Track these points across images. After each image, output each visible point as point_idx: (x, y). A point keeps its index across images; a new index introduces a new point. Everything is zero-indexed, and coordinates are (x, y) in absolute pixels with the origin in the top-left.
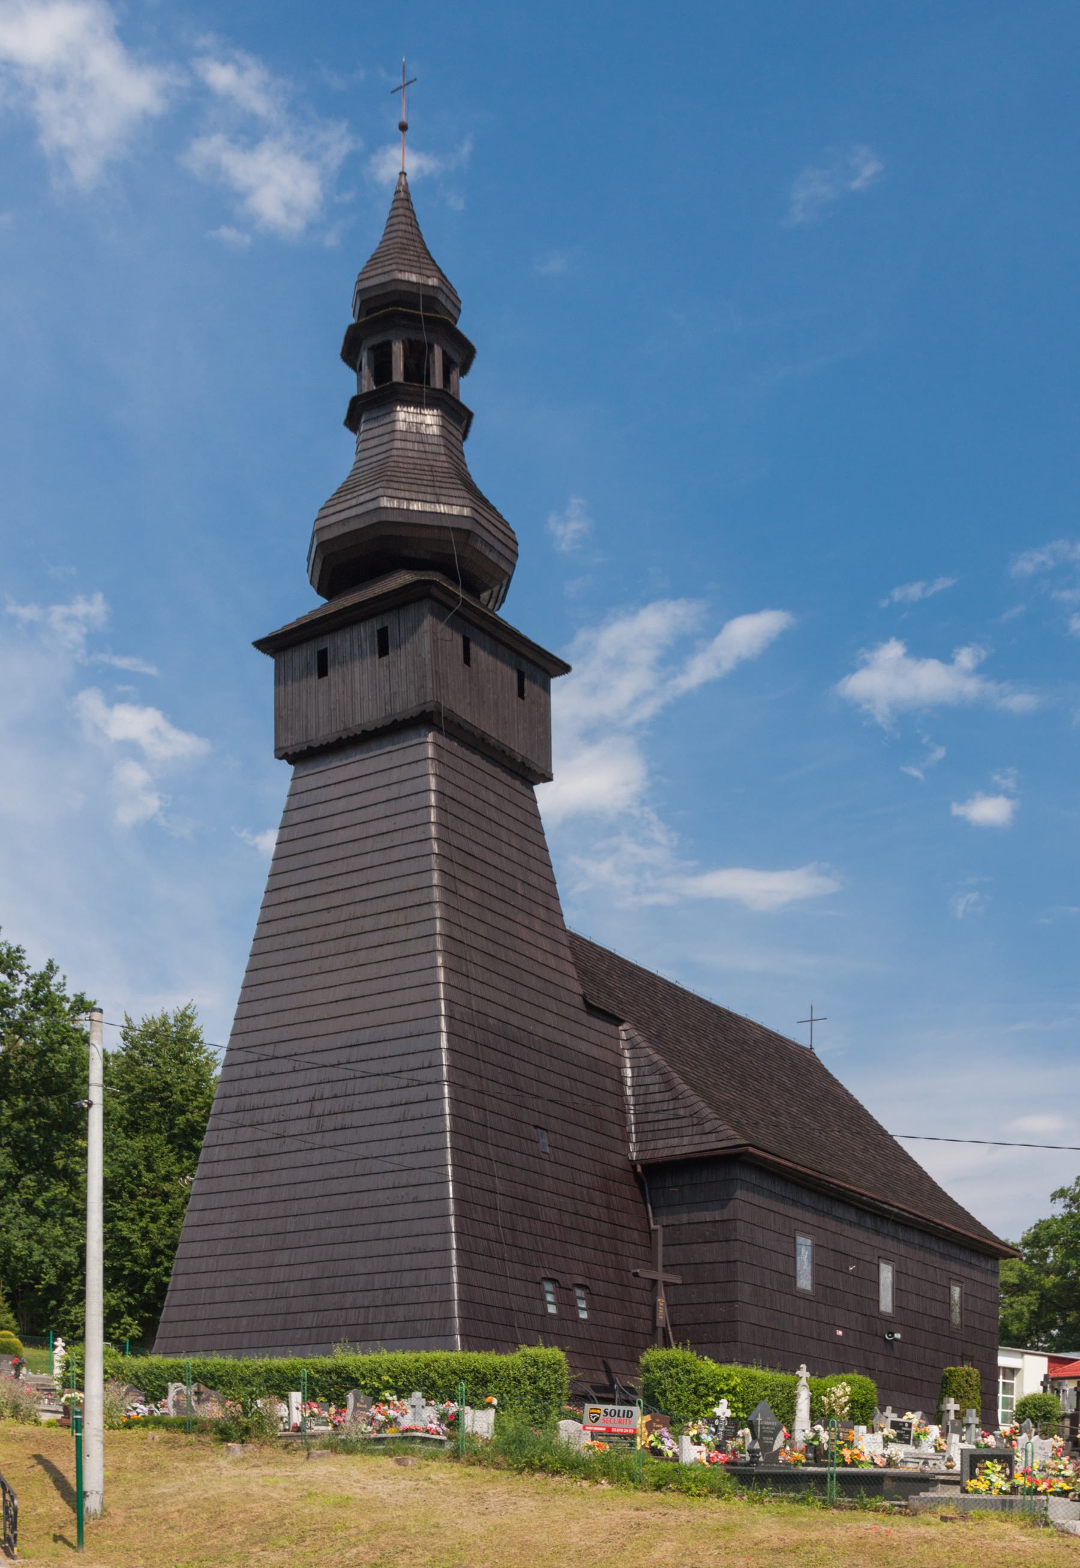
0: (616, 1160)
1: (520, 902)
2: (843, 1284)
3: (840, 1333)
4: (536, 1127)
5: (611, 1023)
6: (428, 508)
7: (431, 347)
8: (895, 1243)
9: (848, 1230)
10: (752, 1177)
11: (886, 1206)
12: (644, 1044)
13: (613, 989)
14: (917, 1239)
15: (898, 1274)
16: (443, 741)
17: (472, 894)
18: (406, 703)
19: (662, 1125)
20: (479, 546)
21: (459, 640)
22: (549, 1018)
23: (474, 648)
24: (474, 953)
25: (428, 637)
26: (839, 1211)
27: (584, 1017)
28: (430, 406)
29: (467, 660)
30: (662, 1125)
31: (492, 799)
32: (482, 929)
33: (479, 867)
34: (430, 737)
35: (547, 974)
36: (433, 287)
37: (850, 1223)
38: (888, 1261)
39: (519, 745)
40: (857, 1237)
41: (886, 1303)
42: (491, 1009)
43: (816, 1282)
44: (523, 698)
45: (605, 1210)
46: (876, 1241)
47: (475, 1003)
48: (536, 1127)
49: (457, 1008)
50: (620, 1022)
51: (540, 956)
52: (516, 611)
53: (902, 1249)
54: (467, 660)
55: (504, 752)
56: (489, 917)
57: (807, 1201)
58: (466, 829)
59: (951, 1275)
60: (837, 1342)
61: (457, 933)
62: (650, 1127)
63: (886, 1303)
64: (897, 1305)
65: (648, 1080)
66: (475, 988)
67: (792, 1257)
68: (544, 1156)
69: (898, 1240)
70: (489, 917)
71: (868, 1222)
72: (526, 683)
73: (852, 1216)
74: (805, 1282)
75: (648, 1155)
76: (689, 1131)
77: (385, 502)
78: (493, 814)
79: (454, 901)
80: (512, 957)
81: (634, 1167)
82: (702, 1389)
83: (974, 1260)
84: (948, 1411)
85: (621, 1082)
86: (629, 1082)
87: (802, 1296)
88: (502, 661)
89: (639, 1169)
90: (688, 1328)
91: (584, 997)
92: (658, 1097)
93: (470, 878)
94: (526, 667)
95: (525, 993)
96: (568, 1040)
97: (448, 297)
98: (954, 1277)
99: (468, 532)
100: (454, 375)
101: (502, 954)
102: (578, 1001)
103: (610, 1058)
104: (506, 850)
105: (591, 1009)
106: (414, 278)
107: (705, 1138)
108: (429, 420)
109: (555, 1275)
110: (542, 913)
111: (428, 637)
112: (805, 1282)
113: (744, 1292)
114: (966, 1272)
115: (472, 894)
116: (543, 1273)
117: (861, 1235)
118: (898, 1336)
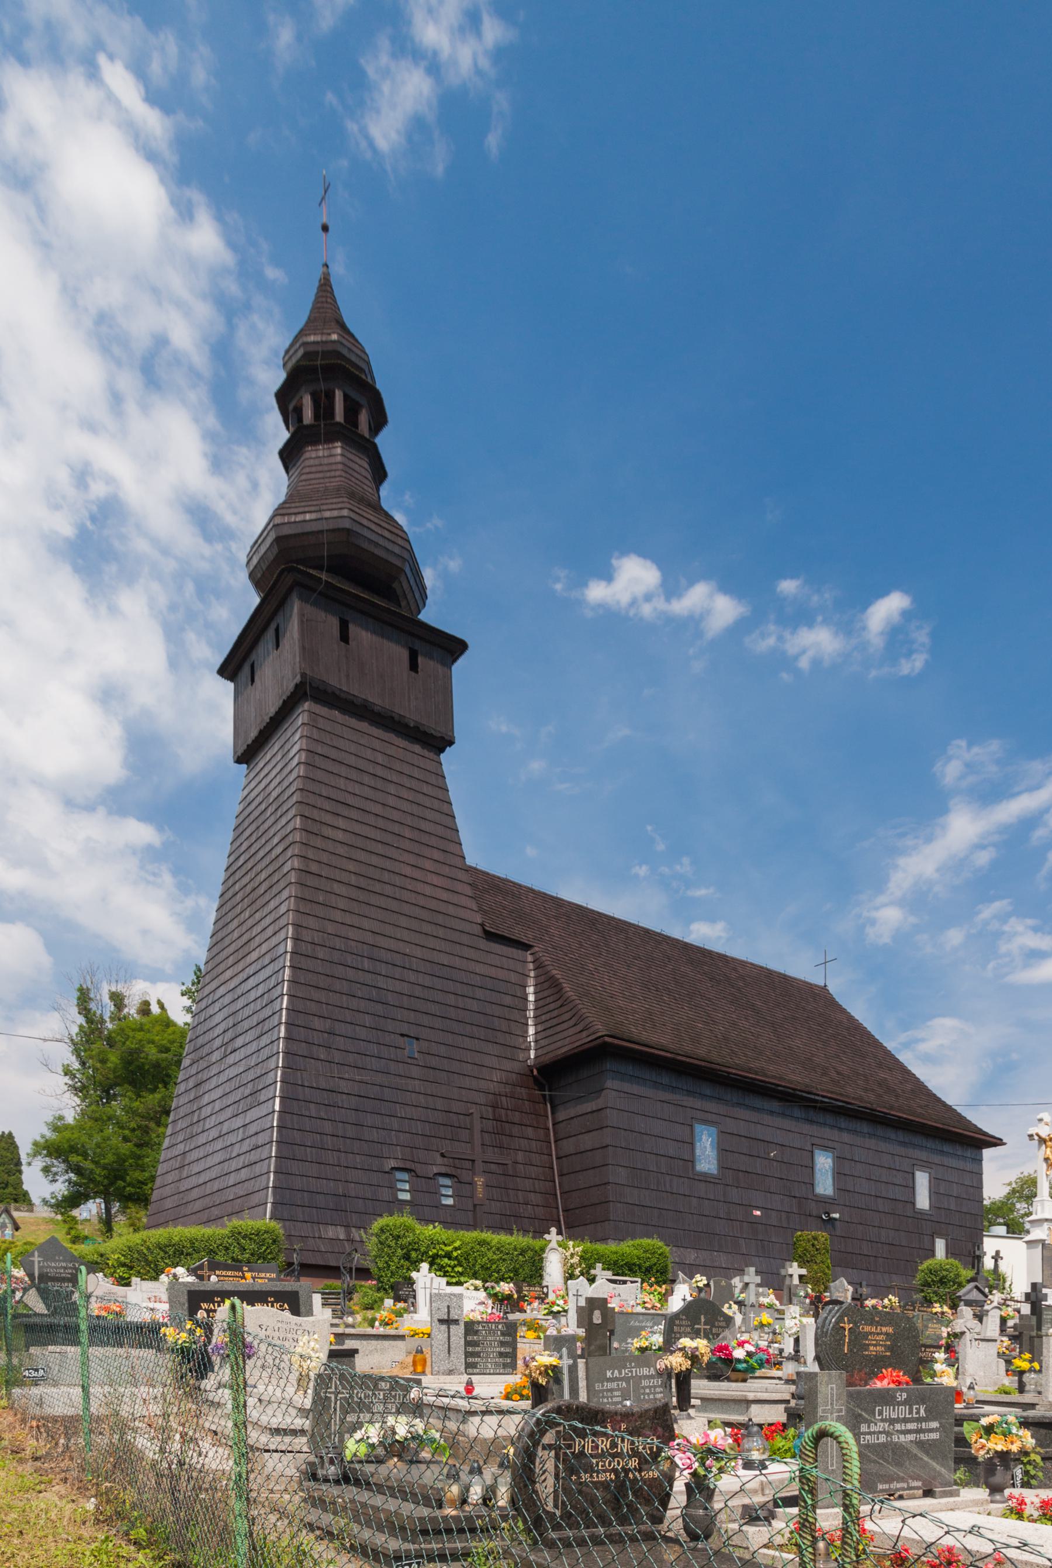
0: (508, 1065)
1: (406, 845)
3: (758, 1213)
4: (402, 1035)
5: (518, 948)
6: (313, 516)
8: (836, 1132)
9: (767, 1119)
11: (813, 1097)
12: (546, 963)
13: (514, 918)
14: (865, 1127)
15: (839, 1160)
17: (340, 836)
20: (365, 545)
22: (431, 943)
23: (353, 629)
24: (335, 885)
27: (483, 944)
28: (330, 439)
29: (345, 637)
31: (380, 758)
32: (351, 866)
33: (354, 814)
35: (433, 904)
36: (334, 342)
37: (772, 1113)
38: (825, 1148)
39: (411, 710)
40: (776, 1128)
42: (352, 933)
43: (722, 1167)
44: (417, 672)
45: (490, 1109)
46: (806, 1128)
47: (330, 928)
48: (402, 1035)
49: (304, 932)
51: (428, 890)
53: (846, 1137)
54: (345, 637)
55: (393, 718)
56: (362, 856)
57: (708, 1092)
58: (342, 783)
59: (915, 1162)
60: (754, 1222)
61: (314, 868)
64: (839, 1189)
65: (546, 994)
66: (338, 916)
68: (409, 1061)
69: (840, 1129)
70: (362, 856)
72: (420, 659)
73: (775, 1105)
76: (571, 1032)
78: (379, 771)
79: (318, 842)
80: (388, 890)
81: (532, 1071)
82: (414, 1254)
83: (947, 1148)
84: (791, 1276)
85: (525, 999)
86: (531, 998)
87: (705, 1178)
88: (389, 639)
89: (535, 1072)
90: (577, 1211)
91: (482, 925)
93: (341, 823)
94: (418, 645)
95: (404, 922)
96: (457, 962)
97: (350, 349)
98: (919, 1163)
99: (348, 531)
101: (378, 887)
102: (478, 930)
103: (513, 977)
104: (391, 801)
105: (490, 936)
106: (318, 338)
107: (578, 1036)
109: (408, 1165)
110: (437, 855)
114: (936, 1159)
115: (340, 836)
116: (393, 1163)
117: (787, 1123)
118: (836, 1216)
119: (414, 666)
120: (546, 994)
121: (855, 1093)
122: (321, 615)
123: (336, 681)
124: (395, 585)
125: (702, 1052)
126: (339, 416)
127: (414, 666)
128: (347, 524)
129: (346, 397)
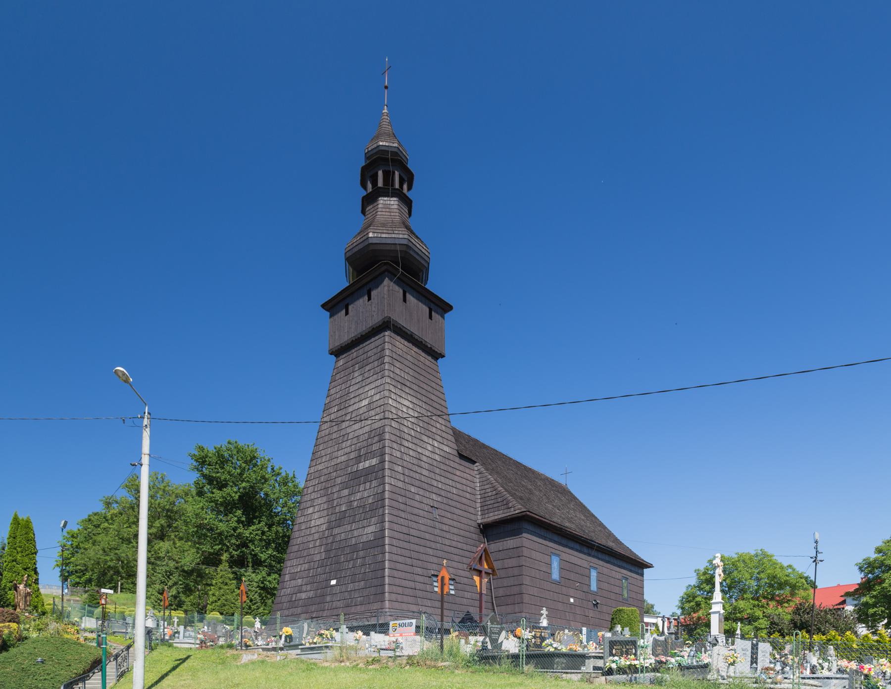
2: (573, 578)
7: (394, 173)
10: (531, 528)
16: (393, 335)
18: (376, 319)
19: (491, 506)
21: (401, 291)
23: (408, 296)
25: (388, 289)
26: (572, 544)
27: (457, 460)
29: (405, 300)
30: (491, 506)
34: (387, 333)
39: (429, 339)
41: (594, 587)
43: (561, 577)
50: (474, 462)
52: (432, 285)
54: (405, 300)
62: (486, 508)
63: (594, 587)
65: (486, 487)
67: (550, 565)
71: (586, 550)
73: (578, 546)
74: (555, 576)
75: (485, 520)
77: (371, 235)
92: (490, 494)
94: (432, 306)
100: (405, 187)
102: (455, 453)
105: (461, 456)
108: (392, 203)
111: (388, 289)
112: (555, 576)
113: (527, 580)
119: (431, 317)
120: (486, 487)
121: (602, 541)
122: (397, 288)
123: (402, 322)
124: (421, 274)
125: (555, 520)
126: (397, 186)
127: (431, 317)
128: (405, 242)
129: (401, 178)
